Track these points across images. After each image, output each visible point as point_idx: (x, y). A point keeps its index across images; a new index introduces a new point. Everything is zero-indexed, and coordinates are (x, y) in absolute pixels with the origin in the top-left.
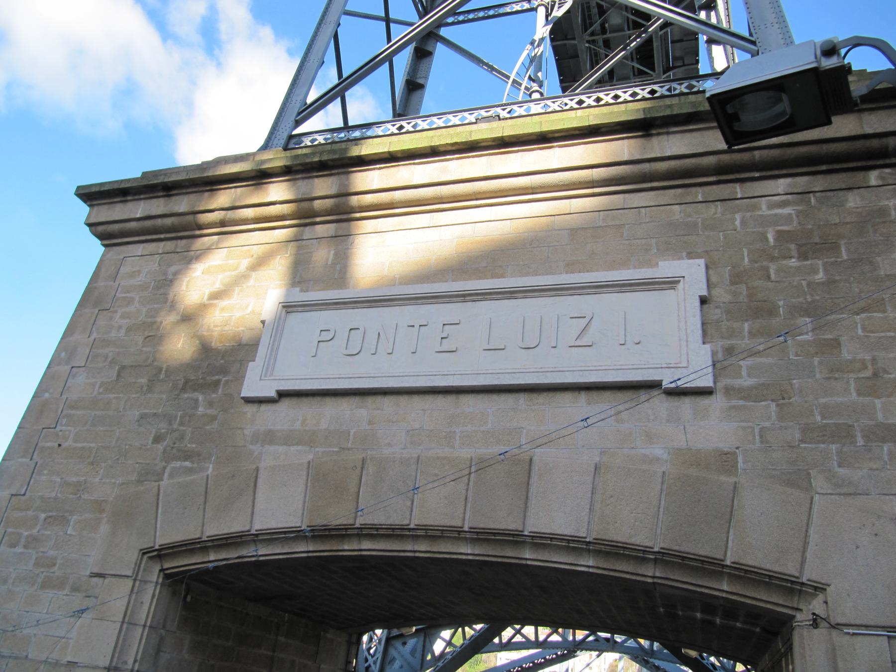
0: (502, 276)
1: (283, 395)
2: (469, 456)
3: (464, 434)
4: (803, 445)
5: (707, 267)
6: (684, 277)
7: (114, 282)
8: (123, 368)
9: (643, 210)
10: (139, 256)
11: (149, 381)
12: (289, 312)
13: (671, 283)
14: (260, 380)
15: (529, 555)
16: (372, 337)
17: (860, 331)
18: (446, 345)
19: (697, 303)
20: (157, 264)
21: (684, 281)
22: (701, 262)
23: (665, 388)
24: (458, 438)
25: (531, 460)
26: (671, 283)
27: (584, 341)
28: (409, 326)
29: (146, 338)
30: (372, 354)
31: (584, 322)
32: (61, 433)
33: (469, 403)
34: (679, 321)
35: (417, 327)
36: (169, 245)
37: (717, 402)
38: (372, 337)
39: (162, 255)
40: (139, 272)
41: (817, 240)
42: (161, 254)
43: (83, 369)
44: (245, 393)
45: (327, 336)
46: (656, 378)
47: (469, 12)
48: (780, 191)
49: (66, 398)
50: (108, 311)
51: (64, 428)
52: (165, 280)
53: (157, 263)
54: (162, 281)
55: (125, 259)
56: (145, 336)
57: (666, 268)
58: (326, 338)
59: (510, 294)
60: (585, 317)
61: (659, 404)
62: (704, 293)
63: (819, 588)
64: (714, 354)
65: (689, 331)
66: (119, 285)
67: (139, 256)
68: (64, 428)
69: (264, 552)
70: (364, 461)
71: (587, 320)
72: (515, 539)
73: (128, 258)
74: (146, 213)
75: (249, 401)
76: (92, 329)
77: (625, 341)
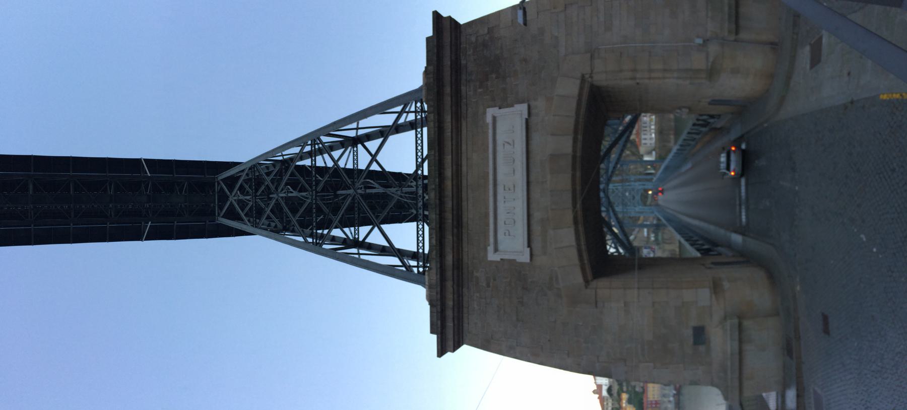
0: (488, 173)
1: (529, 246)
13: (494, 119)
15: (579, 154)
18: (512, 188)
26: (494, 119)
31: (506, 144)
33: (532, 178)
37: (533, 103)
44: (528, 261)
45: (507, 232)
57: (489, 119)
63: (583, 76)
69: (583, 242)
72: (574, 157)
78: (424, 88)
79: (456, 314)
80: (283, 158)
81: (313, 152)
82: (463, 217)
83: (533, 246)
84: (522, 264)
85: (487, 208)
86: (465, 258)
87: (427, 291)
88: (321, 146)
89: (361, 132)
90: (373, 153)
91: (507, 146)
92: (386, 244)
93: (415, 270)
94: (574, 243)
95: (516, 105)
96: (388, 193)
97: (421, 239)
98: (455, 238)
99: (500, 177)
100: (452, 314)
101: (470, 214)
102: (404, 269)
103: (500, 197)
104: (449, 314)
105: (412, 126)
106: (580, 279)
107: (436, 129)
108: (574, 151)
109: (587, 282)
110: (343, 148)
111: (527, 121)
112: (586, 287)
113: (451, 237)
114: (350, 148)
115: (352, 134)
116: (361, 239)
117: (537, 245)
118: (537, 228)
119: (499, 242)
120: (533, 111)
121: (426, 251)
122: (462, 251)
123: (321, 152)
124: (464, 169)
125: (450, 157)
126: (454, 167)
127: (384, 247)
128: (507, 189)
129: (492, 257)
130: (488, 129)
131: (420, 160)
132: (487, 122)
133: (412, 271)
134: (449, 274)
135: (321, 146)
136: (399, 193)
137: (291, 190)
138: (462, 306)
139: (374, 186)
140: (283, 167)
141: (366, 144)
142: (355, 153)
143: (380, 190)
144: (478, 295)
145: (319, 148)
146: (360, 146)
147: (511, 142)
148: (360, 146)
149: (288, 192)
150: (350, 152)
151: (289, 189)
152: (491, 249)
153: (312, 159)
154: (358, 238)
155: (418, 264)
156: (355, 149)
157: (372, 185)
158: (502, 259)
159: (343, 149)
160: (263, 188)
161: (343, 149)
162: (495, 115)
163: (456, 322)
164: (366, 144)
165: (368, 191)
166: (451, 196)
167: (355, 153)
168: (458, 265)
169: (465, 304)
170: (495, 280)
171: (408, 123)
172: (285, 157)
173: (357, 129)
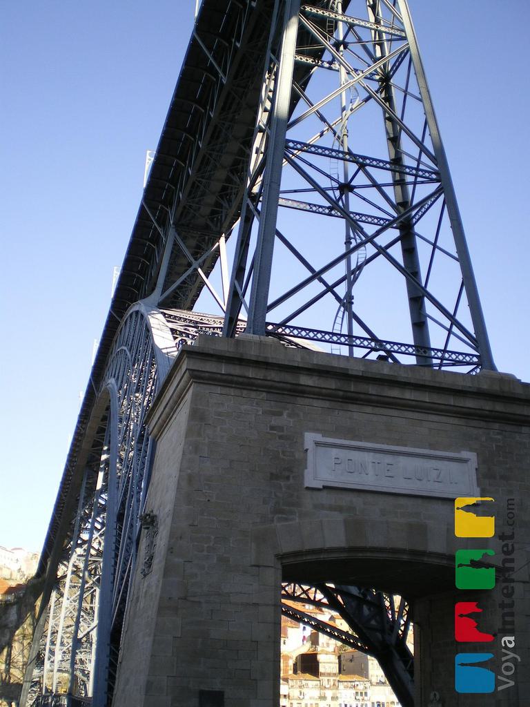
0: (406, 446)
1: (325, 487)
8: (232, 461)
13: (465, 461)
18: (390, 474)
26: (465, 461)
33: (402, 501)
36: (238, 392)
44: (306, 485)
57: (465, 454)
75: (308, 488)
78: (492, 373)
79: (235, 379)
83: (324, 493)
84: (301, 477)
85: (367, 439)
86: (307, 401)
91: (434, 474)
94: (328, 545)
97: (311, 335)
101: (361, 415)
106: (287, 547)
107: (460, 388)
108: (431, 554)
109: (281, 557)
112: (276, 556)
117: (325, 498)
118: (346, 499)
119: (396, 456)
126: (414, 403)
129: (310, 438)
131: (388, 346)
134: (289, 378)
138: (244, 389)
144: (260, 413)
152: (319, 437)
153: (387, 163)
158: (307, 450)
162: (469, 463)
163: (225, 377)
168: (298, 392)
170: (281, 437)
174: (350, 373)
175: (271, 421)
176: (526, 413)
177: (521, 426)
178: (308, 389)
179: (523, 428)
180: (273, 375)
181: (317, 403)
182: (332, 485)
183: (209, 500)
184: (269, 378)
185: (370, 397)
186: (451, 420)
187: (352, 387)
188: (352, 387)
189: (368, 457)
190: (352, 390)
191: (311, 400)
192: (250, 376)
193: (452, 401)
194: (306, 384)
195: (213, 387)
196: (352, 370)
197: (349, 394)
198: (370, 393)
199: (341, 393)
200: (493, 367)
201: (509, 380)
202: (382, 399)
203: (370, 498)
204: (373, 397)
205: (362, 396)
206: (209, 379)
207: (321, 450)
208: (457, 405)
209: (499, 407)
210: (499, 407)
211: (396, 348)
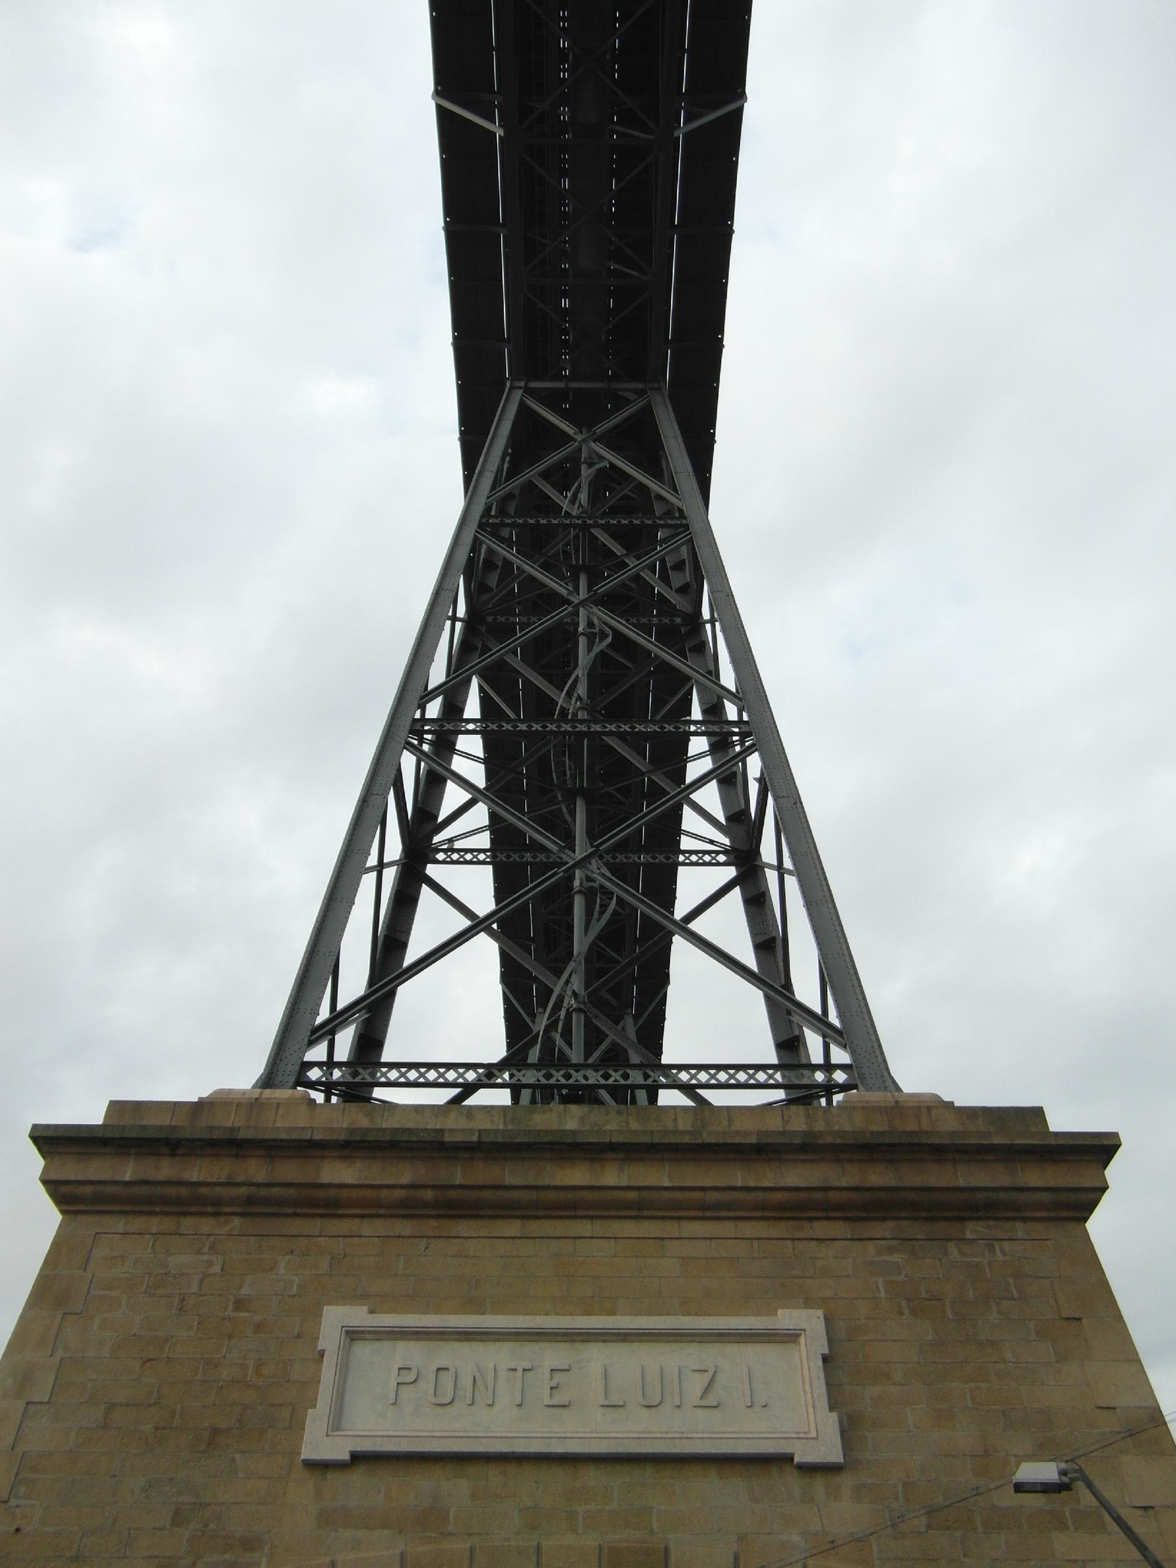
0: (612, 1312)
1: (358, 1458)
2: (597, 1544)
3: (588, 1514)
4: (930, 1532)
5: (826, 1319)
6: (805, 1330)
7: (85, 1270)
8: (112, 1406)
9: (755, 1242)
10: (120, 1234)
11: (157, 1428)
12: (354, 1339)
13: (790, 1337)
14: (327, 1435)
16: (466, 1382)
17: (969, 1402)
18: (558, 1399)
19: (820, 1363)
20: (149, 1250)
21: (805, 1334)
22: (820, 1313)
23: (797, 1463)
24: (580, 1520)
25: (666, 1548)
26: (790, 1337)
27: (711, 1400)
28: (509, 1369)
29: (145, 1362)
30: (469, 1405)
31: (706, 1378)
32: (17, 1511)
33: (592, 1477)
34: (804, 1383)
35: (520, 1372)
36: (168, 1223)
37: (846, 1481)
38: (466, 1382)
39: (157, 1236)
40: (123, 1258)
41: (924, 1295)
42: (155, 1234)
43: (47, 1406)
44: (307, 1453)
45: (411, 1377)
46: (789, 1451)
47: (467, 851)
48: (887, 1235)
49: (21, 1453)
50: (78, 1316)
51: (22, 1502)
52: (165, 1274)
53: (150, 1247)
54: (160, 1277)
55: (98, 1235)
56: (144, 1360)
57: (787, 1318)
58: (407, 1379)
59: (624, 1337)
60: (707, 1371)
61: (794, 1483)
62: (826, 1351)
64: (841, 1422)
65: (815, 1396)
66: (93, 1275)
67: (120, 1234)
68: (22, 1502)
70: (472, 1550)
71: (710, 1374)
73: (102, 1235)
74: (140, 1176)
75: (310, 1465)
76: (55, 1342)
77: (752, 1402)
80: (707, 622)
81: (716, 729)
82: (473, 1223)
83: (357, 1477)
87: (244, 1092)
88: (738, 749)
89: (772, 876)
90: (694, 926)
91: (696, 1384)
92: (410, 958)
93: (318, 1053)
95: (834, 1416)
96: (572, 965)
98: (399, 1194)
99: (596, 1357)
100: (161, 1178)
102: (324, 1013)
103: (529, 1352)
104: (165, 1169)
105: (789, 1045)
107: (753, 1140)
110: (727, 819)
111: (788, 1459)
113: (406, 1179)
114: (727, 841)
115: (767, 851)
116: (431, 870)
120: (819, 1484)
121: (379, 1093)
122: (363, 1216)
123: (719, 746)
124: (629, 1228)
125: (666, 1183)
126: (632, 1195)
127: (403, 946)
128: (559, 1378)
130: (758, 1314)
132: (780, 1312)
133: (312, 1043)
135: (738, 749)
136: (570, 1002)
137: (597, 649)
138: (186, 1214)
139: (593, 922)
140: (678, 620)
141: (736, 893)
142: (707, 858)
143: (580, 942)
144: (217, 1269)
145: (733, 744)
146: (731, 872)
147: (711, 1400)
148: (731, 872)
149: (594, 635)
150: (712, 842)
151: (601, 641)
152: (358, 1315)
154: (437, 862)
155: (340, 1065)
156: (722, 858)
157: (596, 914)
158: (322, 1354)
159: (722, 820)
160: (618, 550)
161: (722, 820)
162: (802, 1340)
163: (135, 1190)
164: (736, 893)
165: (578, 903)
166: (541, 1183)
167: (707, 858)
169: (187, 1223)
171: (797, 1033)
172: (708, 627)
173: (780, 867)
174: (448, 1138)
175: (241, 1287)
176: (962, 1183)
177: (962, 1219)
178: (346, 1193)
179: (970, 1225)
180: (256, 1170)
181: (368, 1228)
182: (378, 1449)
183: (18, 1530)
184: (241, 1179)
185: (508, 1195)
186: (749, 1229)
187: (457, 1174)
188: (457, 1174)
189: (499, 1356)
190: (458, 1182)
191: (357, 1221)
192: (195, 1179)
193: (737, 1176)
194: (337, 1181)
195: (107, 1219)
196: (452, 1131)
197: (452, 1194)
198: (507, 1183)
199: (429, 1195)
200: (887, 1081)
201: (934, 1106)
202: (544, 1195)
203: (493, 1477)
204: (517, 1194)
205: (487, 1195)
206: (97, 1199)
207: (363, 1351)
208: (752, 1184)
209: (878, 1176)
210: (878, 1176)
211: (703, 1077)
